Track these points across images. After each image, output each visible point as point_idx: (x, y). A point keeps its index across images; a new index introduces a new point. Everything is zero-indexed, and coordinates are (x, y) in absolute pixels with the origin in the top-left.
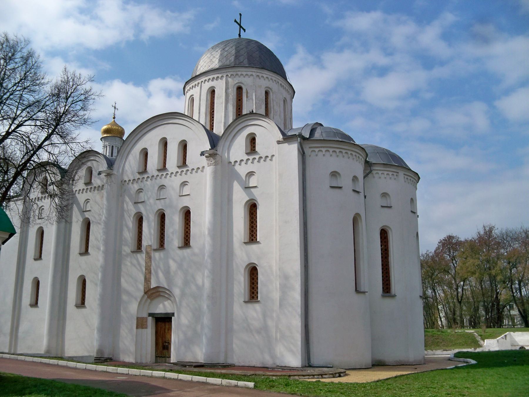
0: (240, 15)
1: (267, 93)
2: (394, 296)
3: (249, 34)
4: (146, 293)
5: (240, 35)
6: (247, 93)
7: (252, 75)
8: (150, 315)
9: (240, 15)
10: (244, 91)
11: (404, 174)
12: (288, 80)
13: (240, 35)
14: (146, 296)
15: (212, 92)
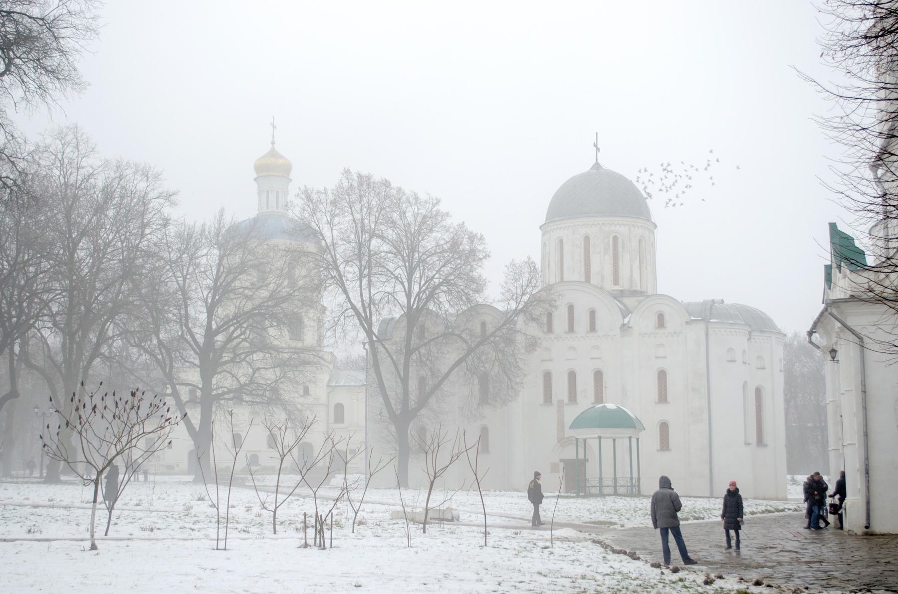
0: (597, 133)
1: (640, 241)
2: (766, 446)
3: (611, 163)
4: (558, 442)
5: (597, 159)
6: (623, 243)
7: (628, 225)
8: (561, 460)
9: (597, 133)
10: (620, 241)
11: (776, 338)
12: (653, 221)
13: (597, 159)
14: (559, 445)
15: (587, 239)
